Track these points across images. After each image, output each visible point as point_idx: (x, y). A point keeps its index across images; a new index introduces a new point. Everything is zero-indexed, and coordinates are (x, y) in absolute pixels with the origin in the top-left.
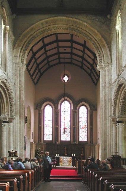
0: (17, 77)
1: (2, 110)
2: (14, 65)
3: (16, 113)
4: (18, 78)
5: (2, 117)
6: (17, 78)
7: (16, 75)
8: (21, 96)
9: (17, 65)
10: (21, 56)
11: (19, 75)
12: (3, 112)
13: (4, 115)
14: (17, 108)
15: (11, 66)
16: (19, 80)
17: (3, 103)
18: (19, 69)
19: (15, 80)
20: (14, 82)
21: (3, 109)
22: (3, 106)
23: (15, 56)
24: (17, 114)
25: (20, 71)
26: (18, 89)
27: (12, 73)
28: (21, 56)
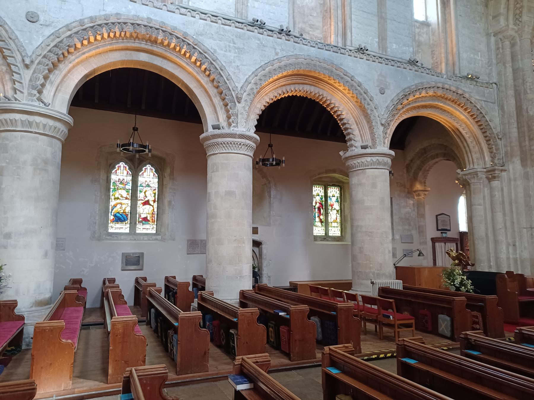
0: (504, 64)
1: (465, 155)
2: (493, 39)
3: (509, 155)
4: (509, 65)
5: (470, 171)
6: (505, 68)
7: (501, 62)
8: (525, 107)
9: (500, 36)
10: (512, 6)
11: (509, 58)
12: (469, 161)
13: (472, 166)
14: (511, 143)
15: (483, 47)
16: (509, 70)
17: (463, 139)
18: (507, 43)
19: (499, 74)
20: (495, 81)
21: (467, 153)
22: (465, 148)
23: (494, 17)
24: (512, 156)
25: (513, 45)
26: (511, 92)
27: (488, 62)
28: (512, 6)
